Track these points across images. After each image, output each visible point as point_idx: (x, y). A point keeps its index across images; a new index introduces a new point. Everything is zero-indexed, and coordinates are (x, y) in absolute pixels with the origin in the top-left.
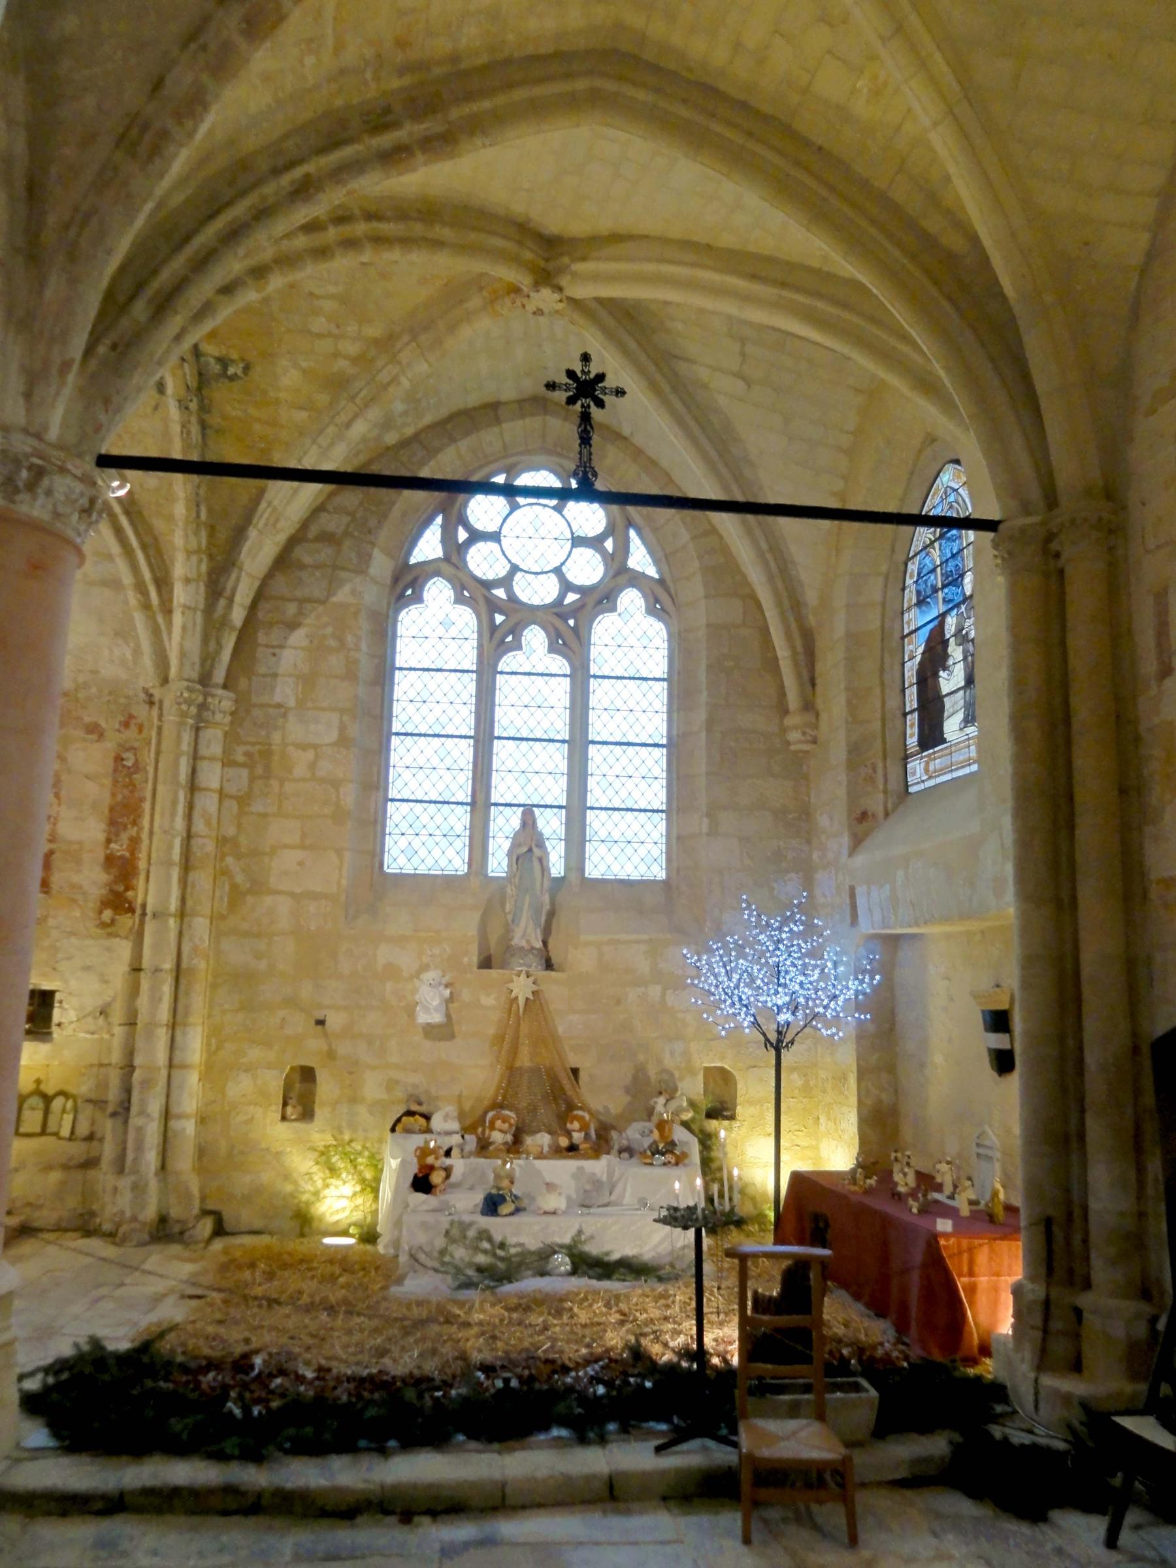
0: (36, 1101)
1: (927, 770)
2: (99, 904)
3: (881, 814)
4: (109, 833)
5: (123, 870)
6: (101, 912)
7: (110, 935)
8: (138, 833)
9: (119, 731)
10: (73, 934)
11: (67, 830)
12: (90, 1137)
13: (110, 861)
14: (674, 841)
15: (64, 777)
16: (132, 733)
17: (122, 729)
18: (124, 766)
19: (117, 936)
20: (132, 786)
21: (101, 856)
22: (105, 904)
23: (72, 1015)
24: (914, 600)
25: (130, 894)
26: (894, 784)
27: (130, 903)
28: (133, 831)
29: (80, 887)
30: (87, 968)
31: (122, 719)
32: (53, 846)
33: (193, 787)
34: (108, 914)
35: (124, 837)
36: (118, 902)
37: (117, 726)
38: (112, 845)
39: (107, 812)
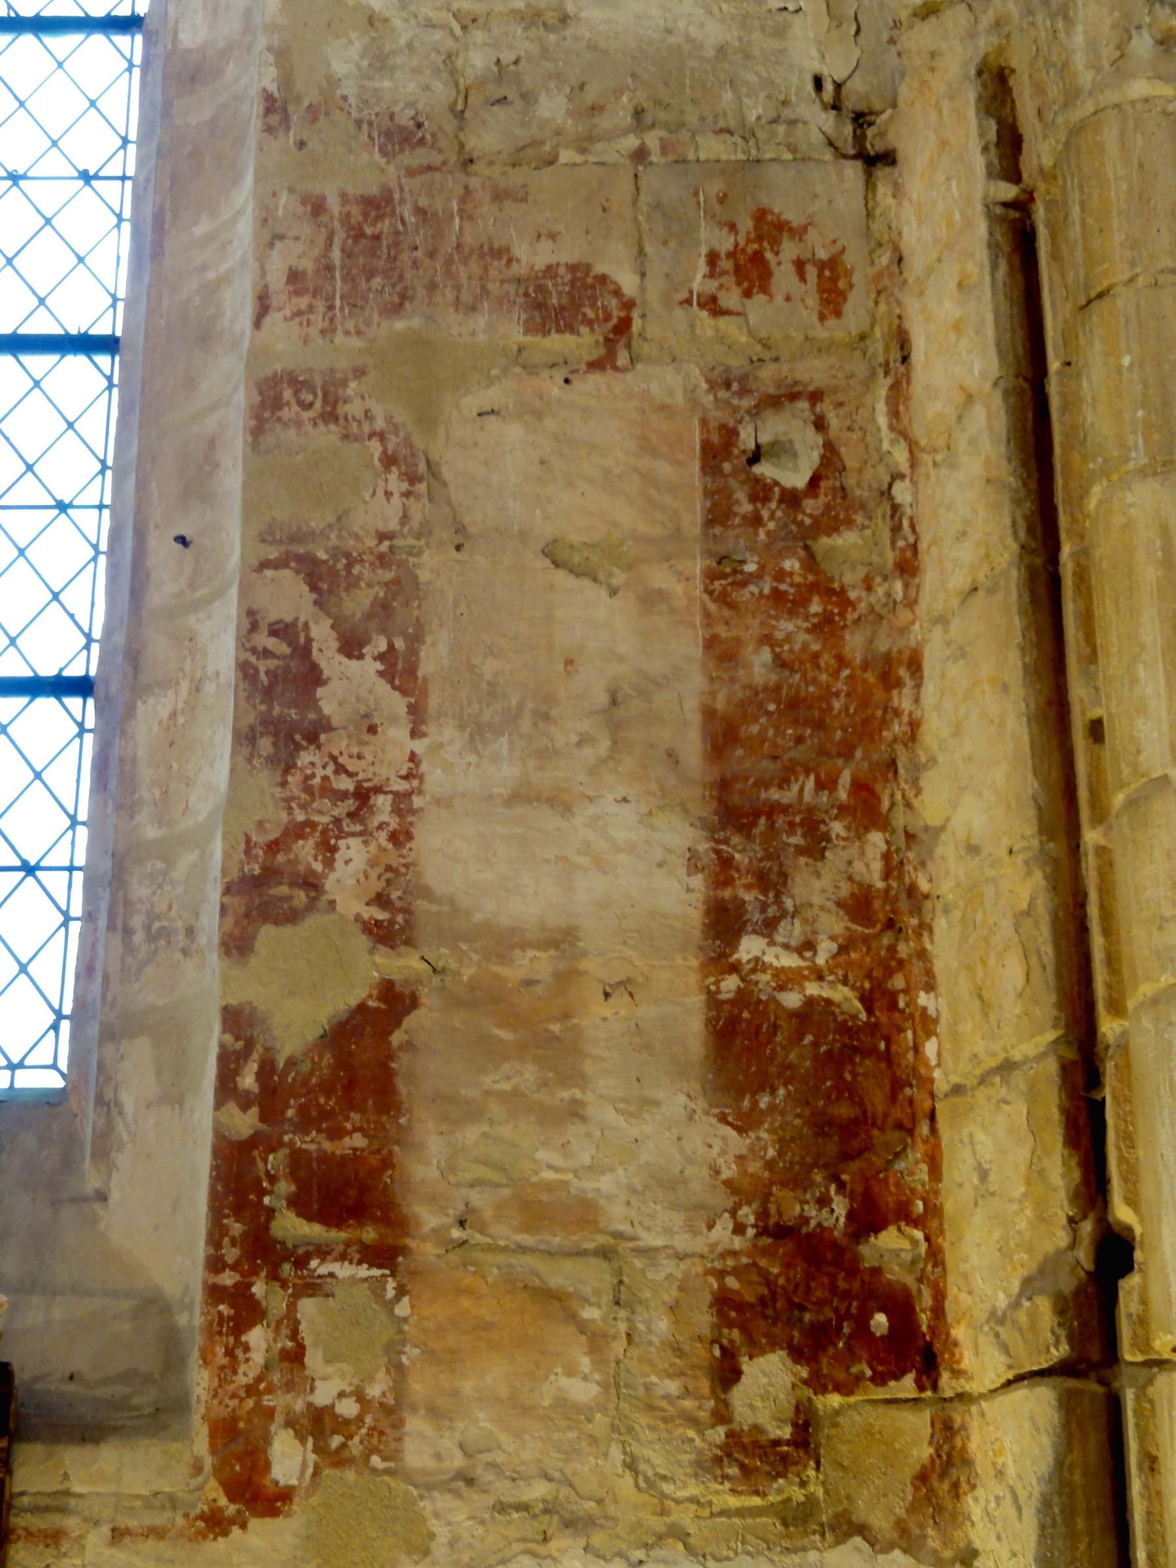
2: (704, 1319)
4: (723, 870)
5: (830, 1090)
6: (727, 1373)
7: (798, 1519)
8: (892, 866)
9: (712, 305)
11: (472, 862)
13: (742, 1042)
15: (430, 566)
16: (783, 313)
17: (731, 298)
18: (761, 491)
19: (847, 1527)
21: (680, 1007)
22: (745, 1317)
25: (892, 1246)
27: (901, 1307)
28: (867, 859)
29: (585, 1213)
31: (726, 243)
32: (403, 965)
34: (768, 1382)
35: (816, 888)
37: (699, 282)
38: (750, 947)
39: (693, 747)
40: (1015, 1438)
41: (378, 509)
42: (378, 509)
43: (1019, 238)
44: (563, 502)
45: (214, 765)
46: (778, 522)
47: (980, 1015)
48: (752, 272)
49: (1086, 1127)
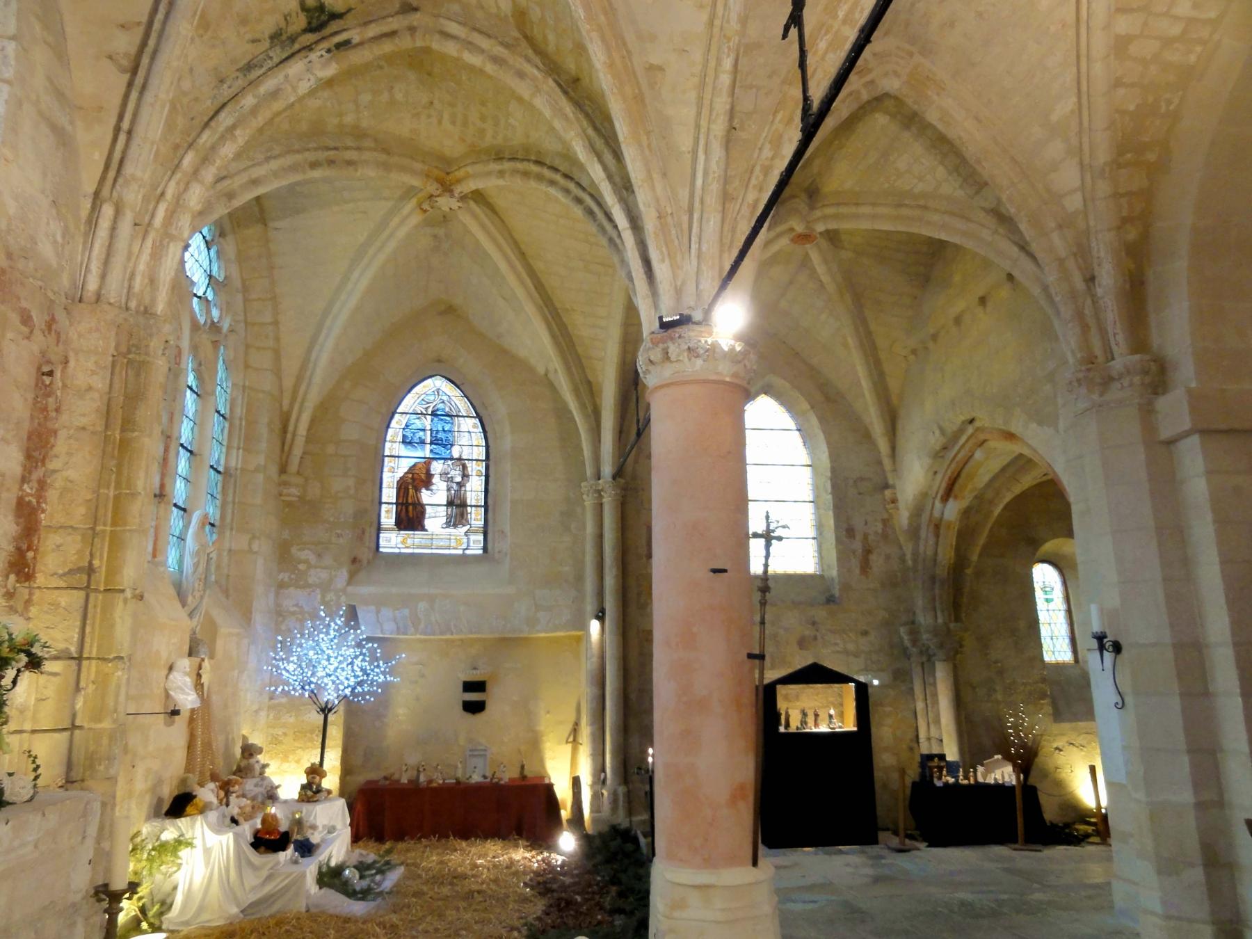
1: (403, 542)
3: (365, 562)
4: (24, 467)
6: (7, 577)
14: (225, 554)
24: (400, 438)
25: (30, 554)
26: (373, 546)
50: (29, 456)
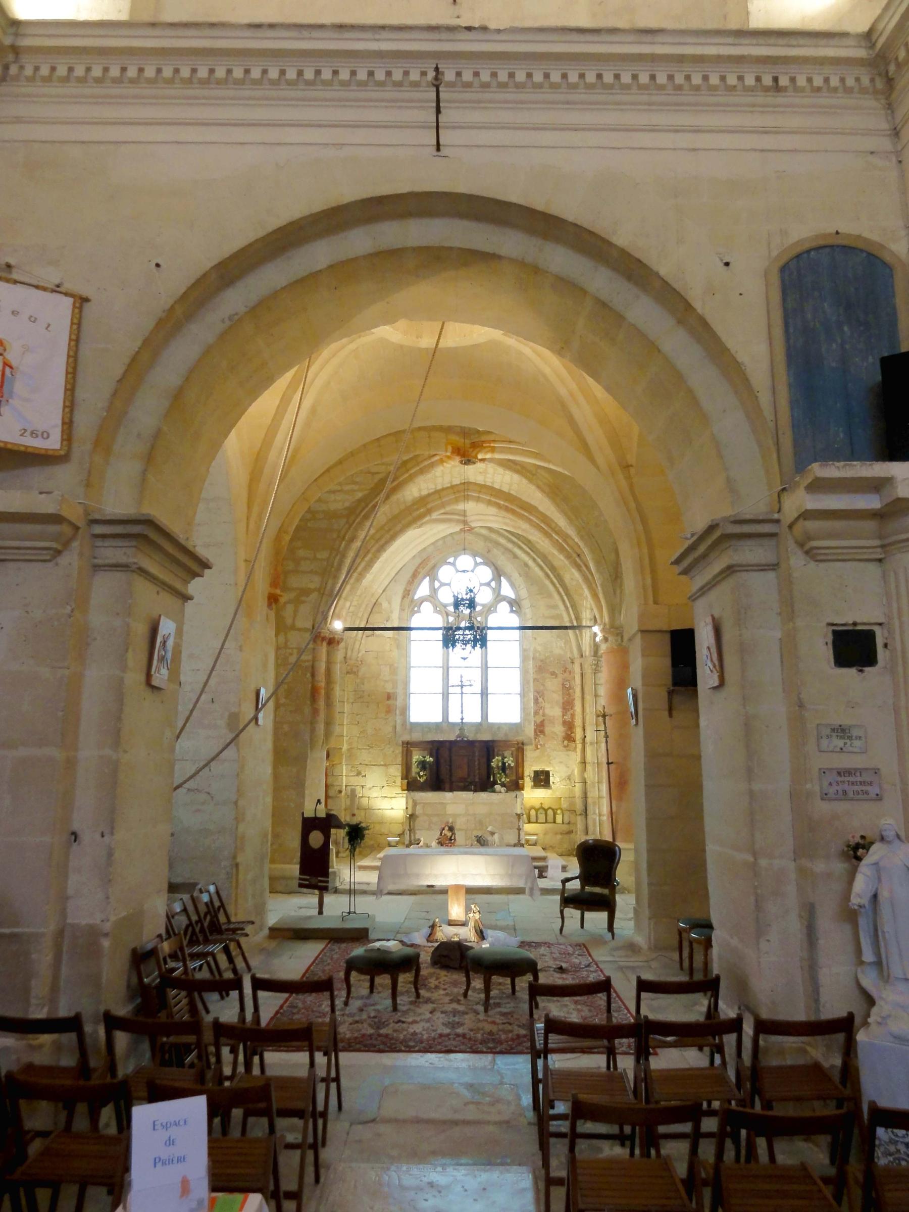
0: (541, 811)
5: (569, 726)
10: (554, 750)
12: (569, 823)
13: (565, 723)
16: (567, 675)
20: (569, 695)
21: (561, 721)
23: (558, 779)
30: (561, 762)
33: (596, 696)
34: (566, 742)
35: (569, 713)
36: (569, 738)
40: (579, 746)
41: (542, 688)
42: (542, 688)
43: (582, 675)
44: (553, 685)
45: (532, 704)
46: (567, 689)
47: (578, 722)
48: (565, 671)
49: (584, 730)
50: (564, 708)
